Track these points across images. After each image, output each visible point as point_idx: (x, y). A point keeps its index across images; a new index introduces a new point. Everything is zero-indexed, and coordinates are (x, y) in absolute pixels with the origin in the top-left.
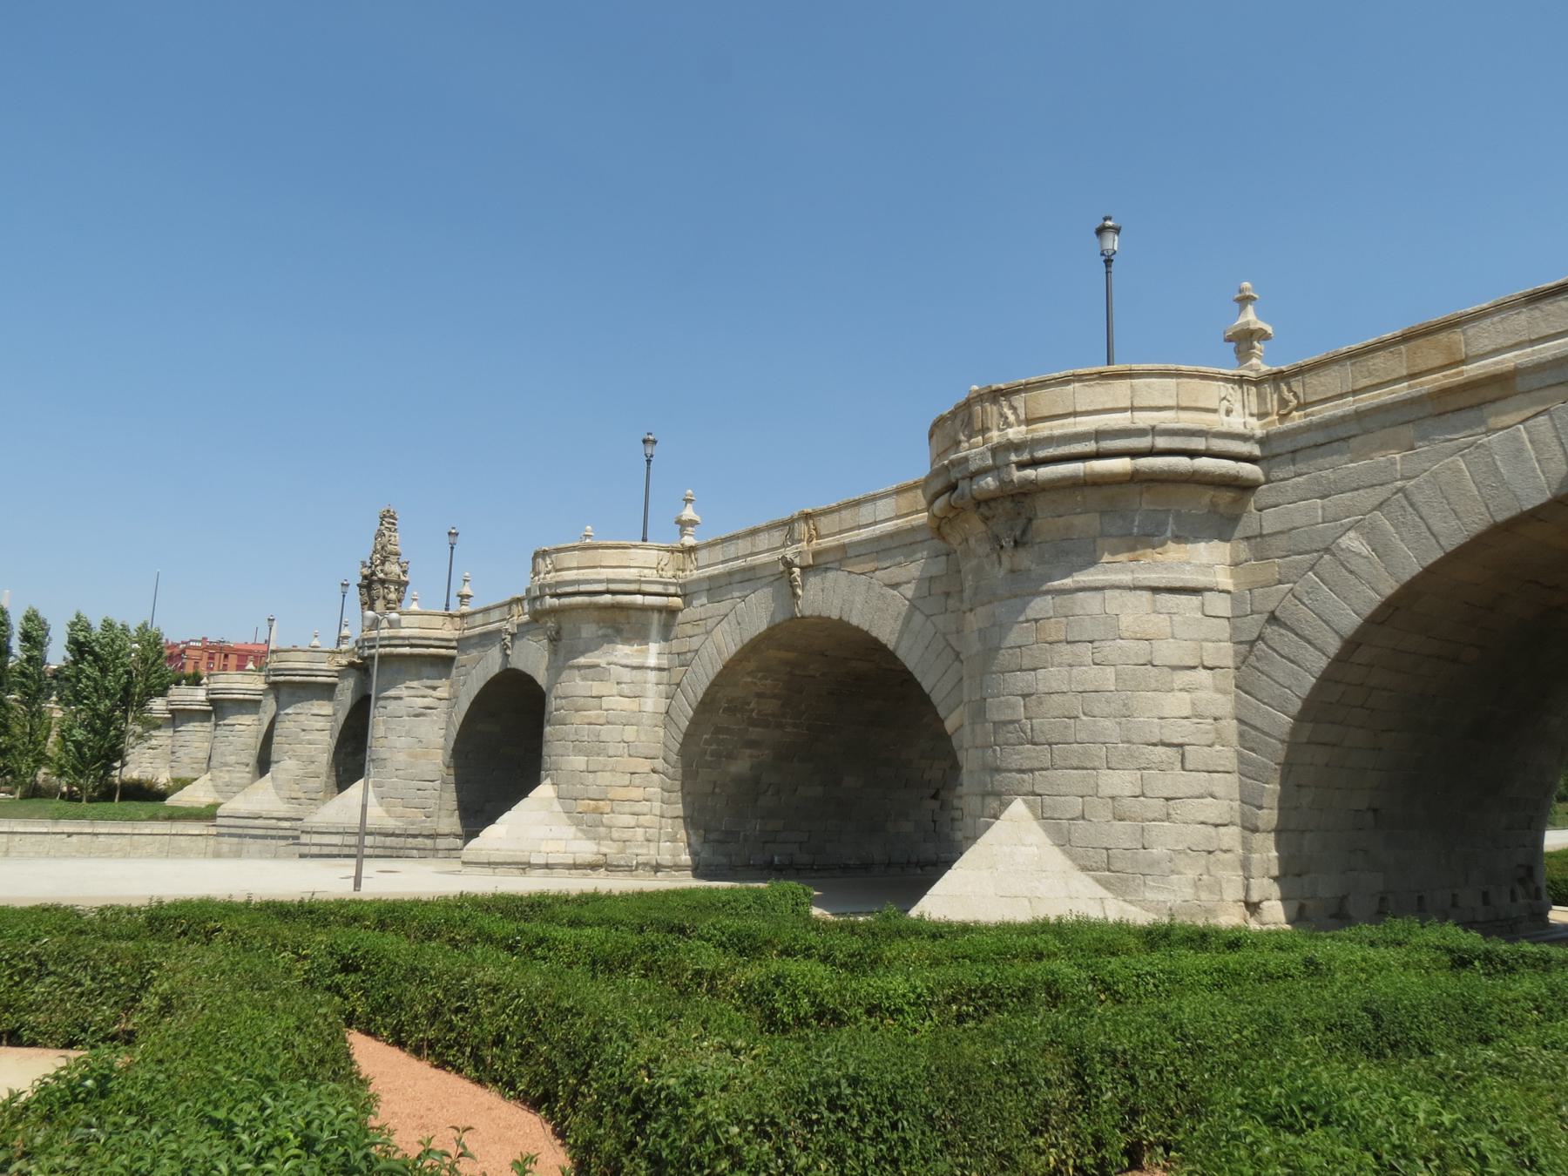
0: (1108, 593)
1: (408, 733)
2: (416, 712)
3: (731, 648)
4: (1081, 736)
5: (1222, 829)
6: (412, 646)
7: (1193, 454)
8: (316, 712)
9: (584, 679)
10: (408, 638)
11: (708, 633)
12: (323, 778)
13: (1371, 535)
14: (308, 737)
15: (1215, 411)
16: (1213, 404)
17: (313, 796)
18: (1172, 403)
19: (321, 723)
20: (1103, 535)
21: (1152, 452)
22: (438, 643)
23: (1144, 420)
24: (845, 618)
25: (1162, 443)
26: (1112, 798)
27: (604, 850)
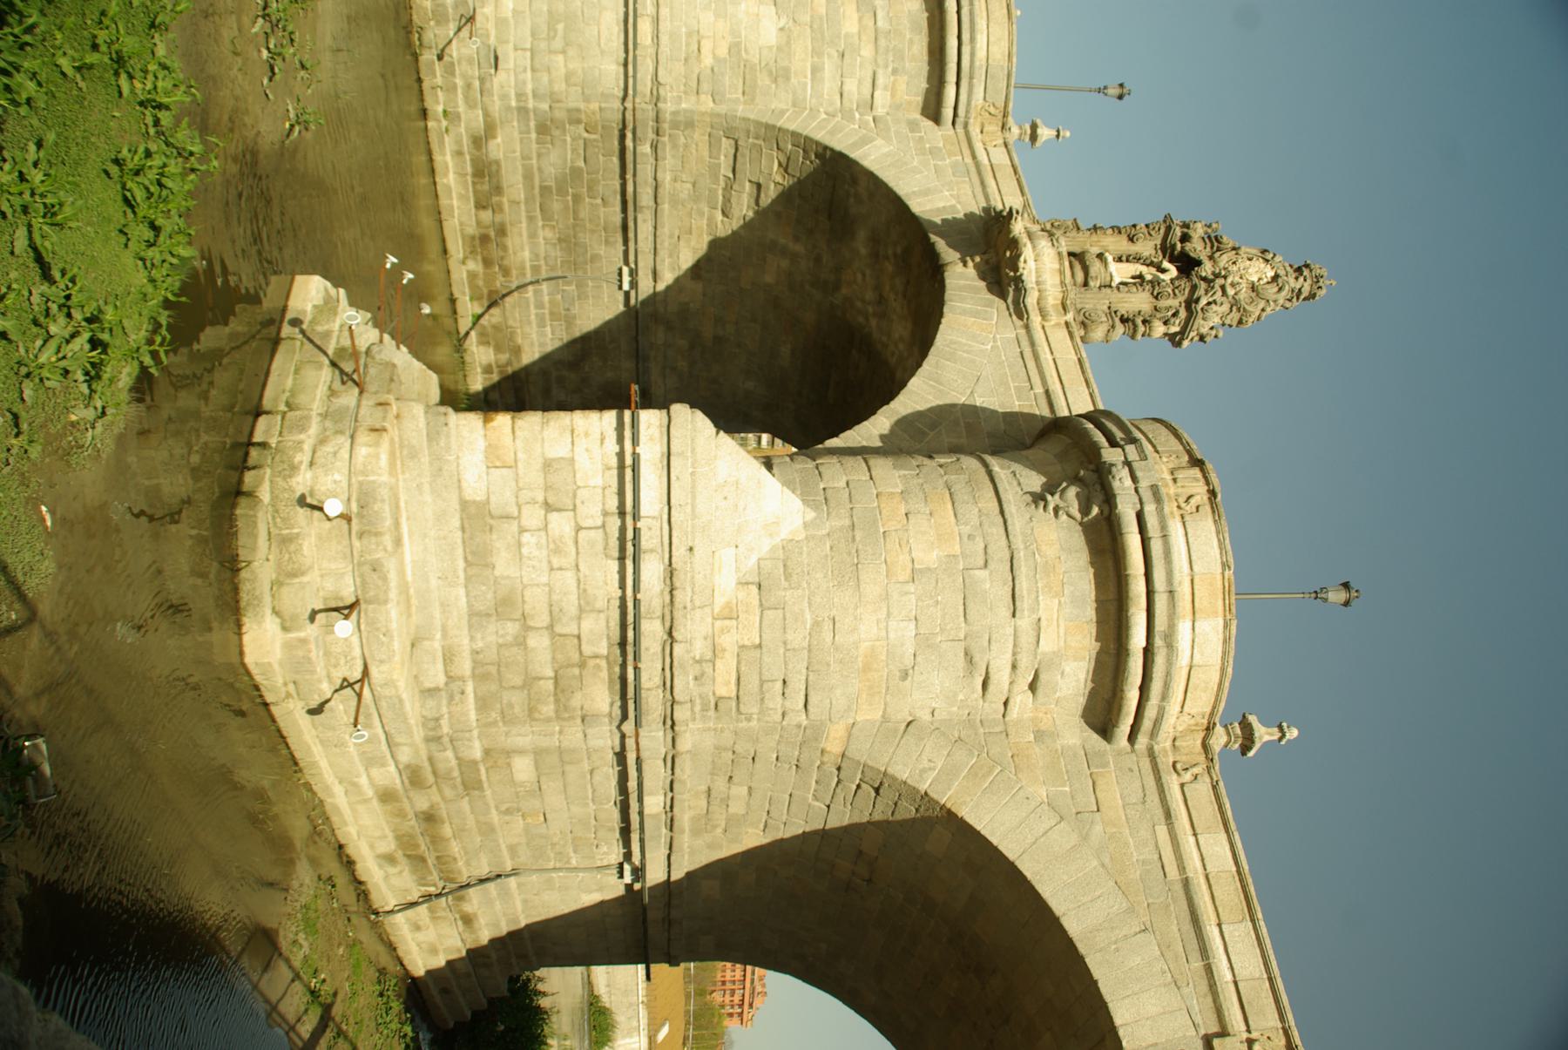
1: (924, 642)
2: (976, 659)
6: (1148, 652)
8: (880, 81)
10: (1170, 646)
12: (741, 111)
17: (705, 86)
19: (855, 88)
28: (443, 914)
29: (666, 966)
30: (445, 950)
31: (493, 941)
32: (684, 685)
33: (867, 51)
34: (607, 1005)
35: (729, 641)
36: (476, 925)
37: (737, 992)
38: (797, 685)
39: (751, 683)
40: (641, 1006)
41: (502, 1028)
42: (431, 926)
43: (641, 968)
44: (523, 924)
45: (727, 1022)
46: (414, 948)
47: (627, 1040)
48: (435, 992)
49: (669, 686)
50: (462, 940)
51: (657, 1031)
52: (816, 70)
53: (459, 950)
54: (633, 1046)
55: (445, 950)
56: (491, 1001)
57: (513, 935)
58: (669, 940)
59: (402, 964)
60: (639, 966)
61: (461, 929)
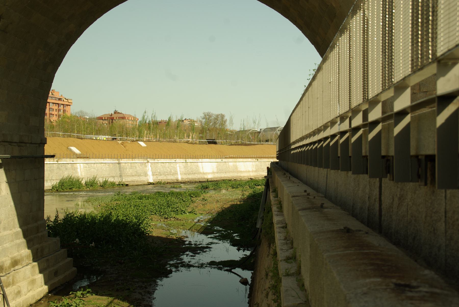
28: (11, 278)
29: (46, 147)
30: (33, 275)
31: (29, 248)
34: (58, 181)
36: (19, 258)
37: (51, 106)
40: (59, 162)
41: (77, 240)
42: (18, 284)
43: (47, 161)
44: (19, 230)
45: (68, 114)
46: (30, 294)
47: (79, 170)
48: (56, 280)
50: (27, 265)
51: (74, 153)
53: (33, 267)
54: (82, 167)
55: (33, 275)
56: (62, 247)
57: (26, 235)
58: (31, 143)
59: (40, 300)
60: (45, 162)
61: (20, 267)
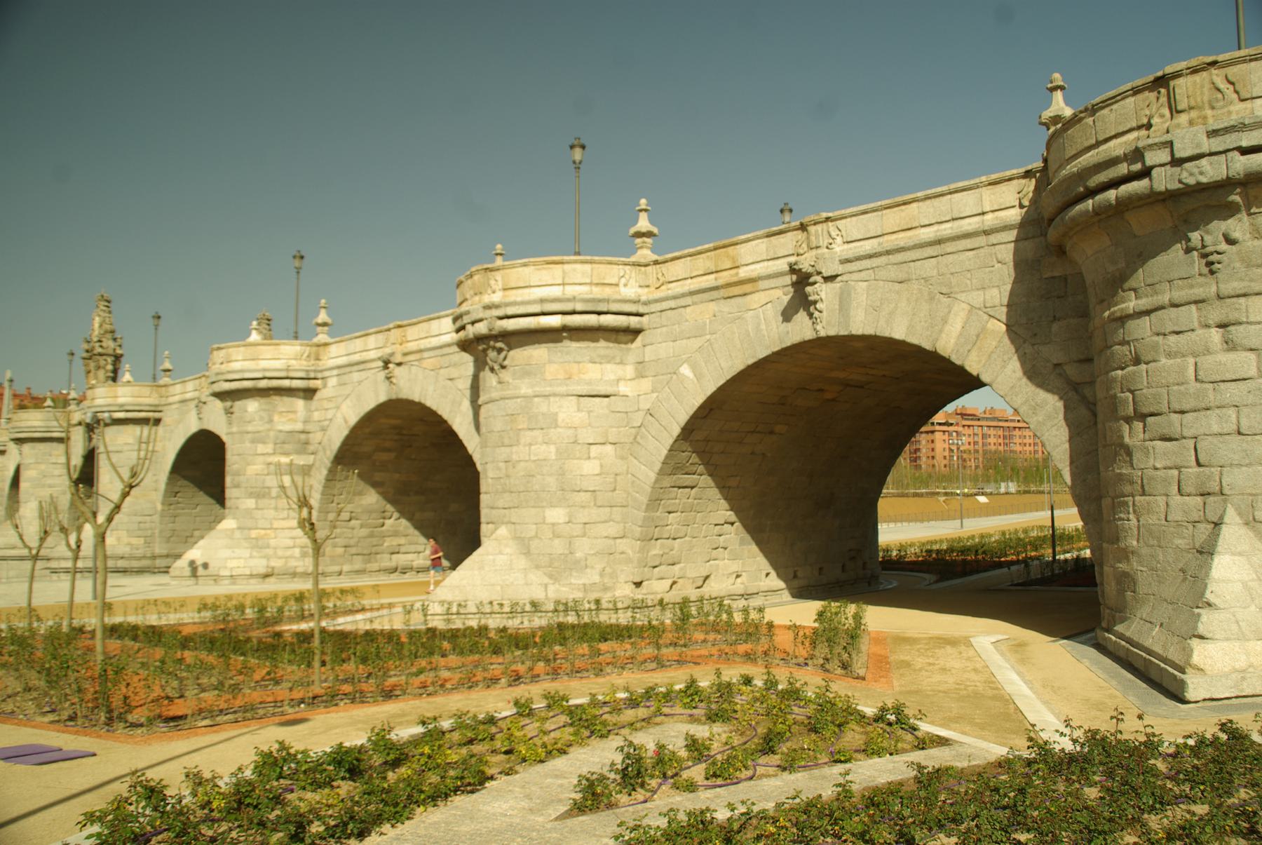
0: (552, 399)
3: (353, 420)
4: (537, 487)
5: (618, 541)
7: (599, 313)
8: (54, 461)
9: (253, 441)
11: (338, 408)
13: (694, 368)
14: (49, 481)
15: (617, 285)
16: (614, 281)
18: (588, 281)
20: (550, 362)
21: (574, 313)
22: (147, 408)
23: (570, 291)
24: (423, 401)
25: (579, 307)
26: (553, 524)
27: (273, 564)
32: (139, 553)
33: (43, 467)
35: (126, 540)
38: (140, 519)
39: (140, 533)
49: (140, 559)
52: (50, 486)
